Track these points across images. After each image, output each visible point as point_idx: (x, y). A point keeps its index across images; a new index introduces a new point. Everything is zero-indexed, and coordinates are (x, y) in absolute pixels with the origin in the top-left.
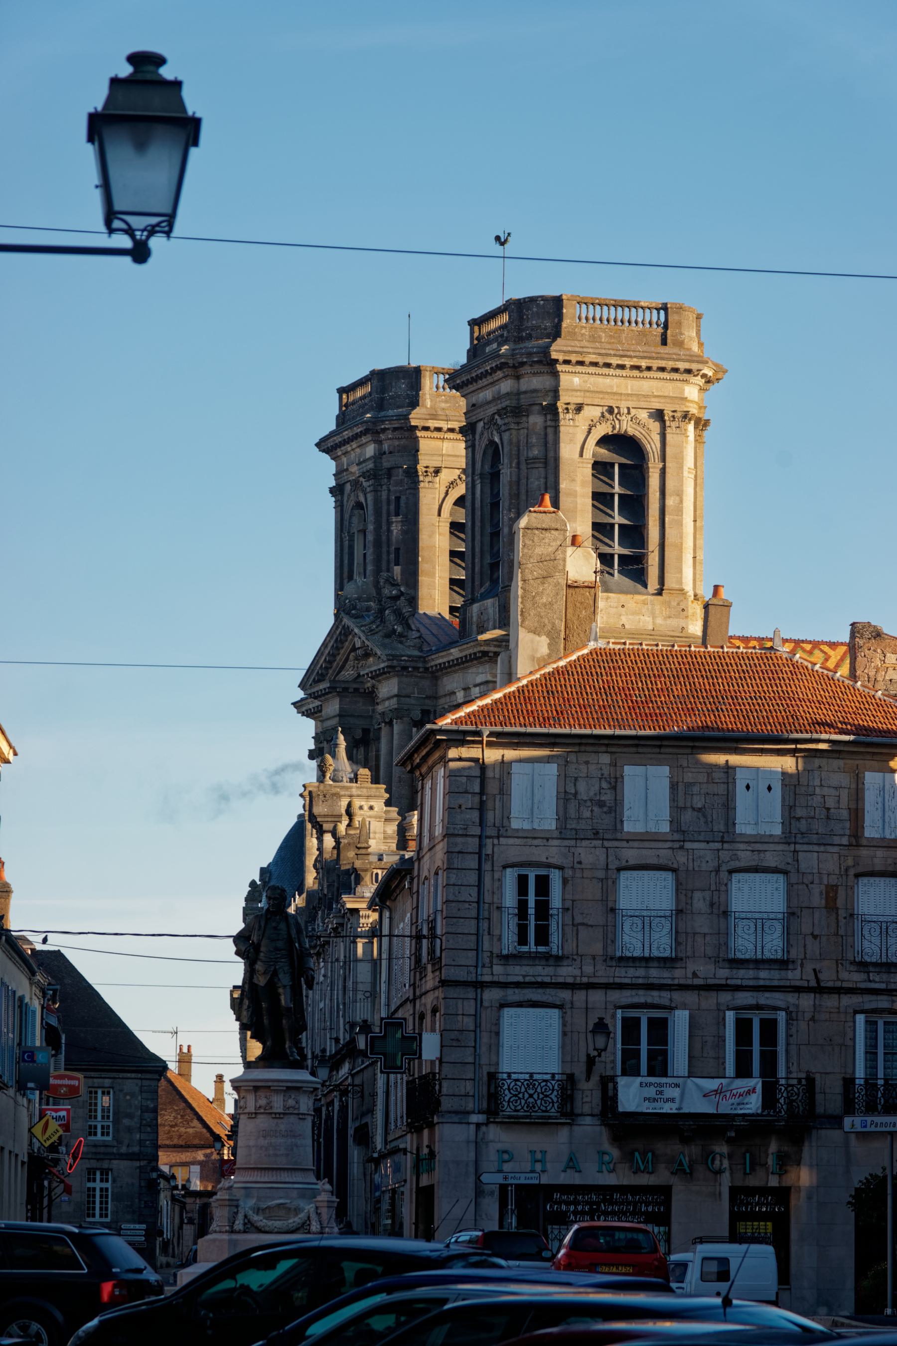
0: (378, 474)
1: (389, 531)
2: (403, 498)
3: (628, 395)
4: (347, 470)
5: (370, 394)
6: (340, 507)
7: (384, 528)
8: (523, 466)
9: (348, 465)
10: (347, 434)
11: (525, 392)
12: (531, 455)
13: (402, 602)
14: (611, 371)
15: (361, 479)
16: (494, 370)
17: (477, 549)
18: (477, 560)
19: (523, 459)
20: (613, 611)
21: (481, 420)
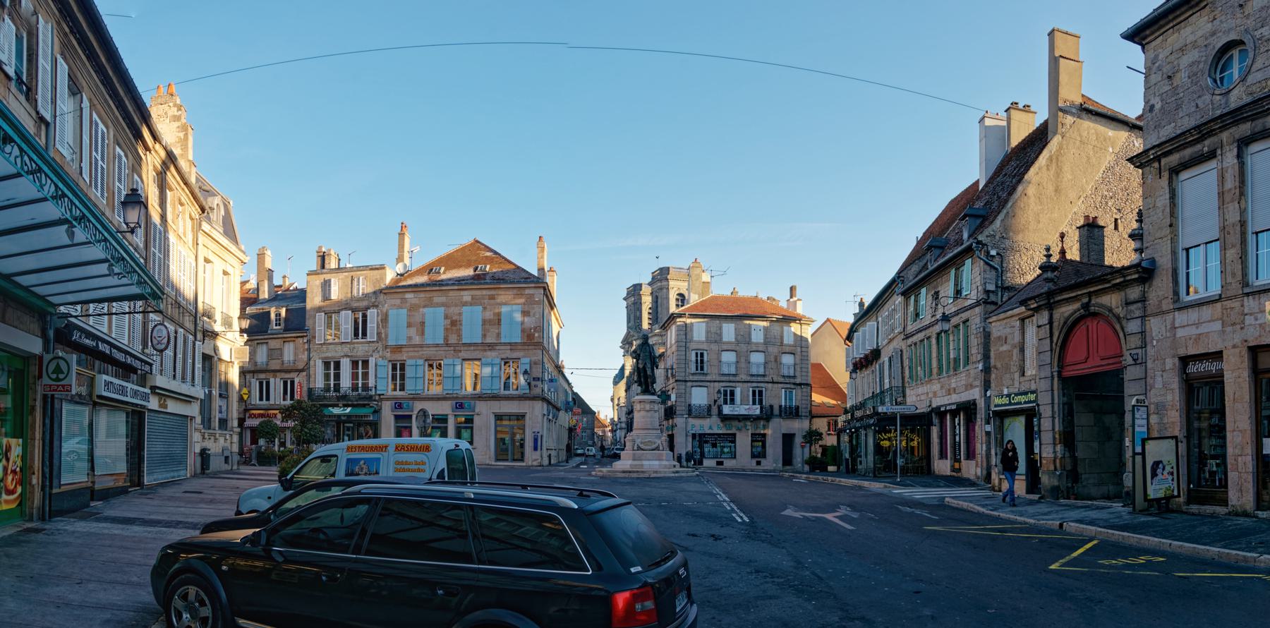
0: (635, 303)
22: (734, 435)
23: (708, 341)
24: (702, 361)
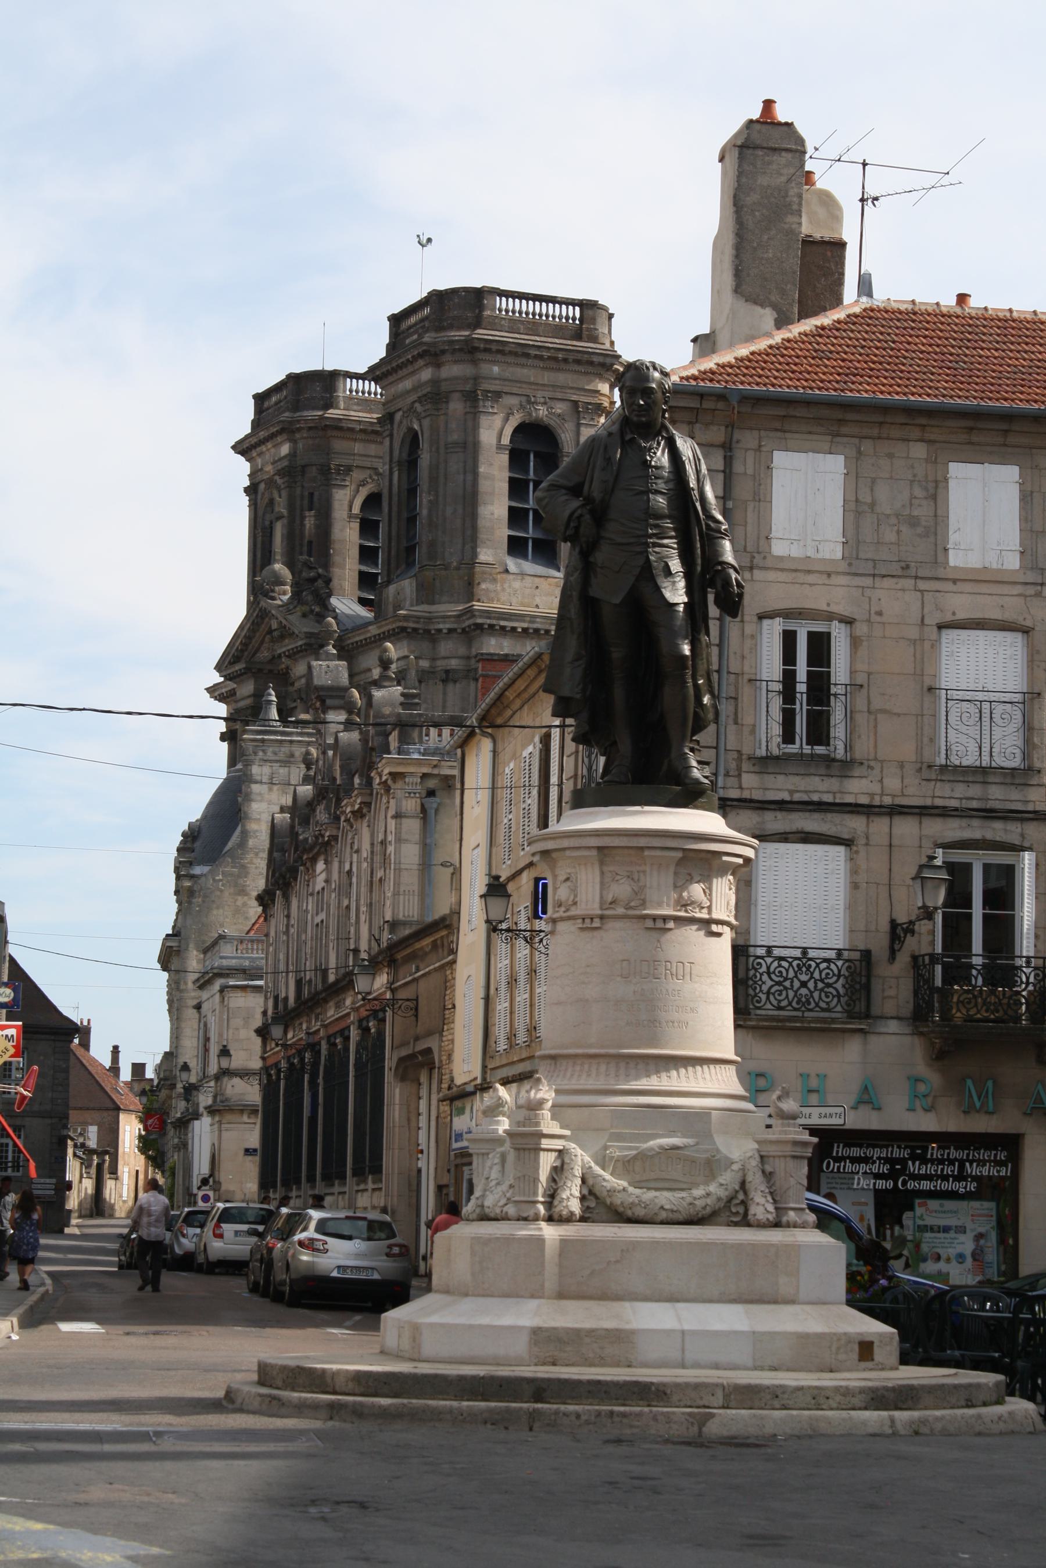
0: (292, 471)
1: (302, 525)
2: (316, 494)
3: (544, 385)
4: (261, 469)
5: (286, 397)
6: (254, 505)
7: (298, 522)
8: (442, 450)
9: (263, 465)
10: (262, 434)
11: (446, 380)
12: (450, 439)
13: (320, 583)
14: (530, 362)
15: (277, 478)
16: (415, 359)
17: (394, 533)
18: (393, 544)
20: (527, 591)
21: (399, 410)
22: (1010, 1145)
23: (860, 560)
24: (820, 687)
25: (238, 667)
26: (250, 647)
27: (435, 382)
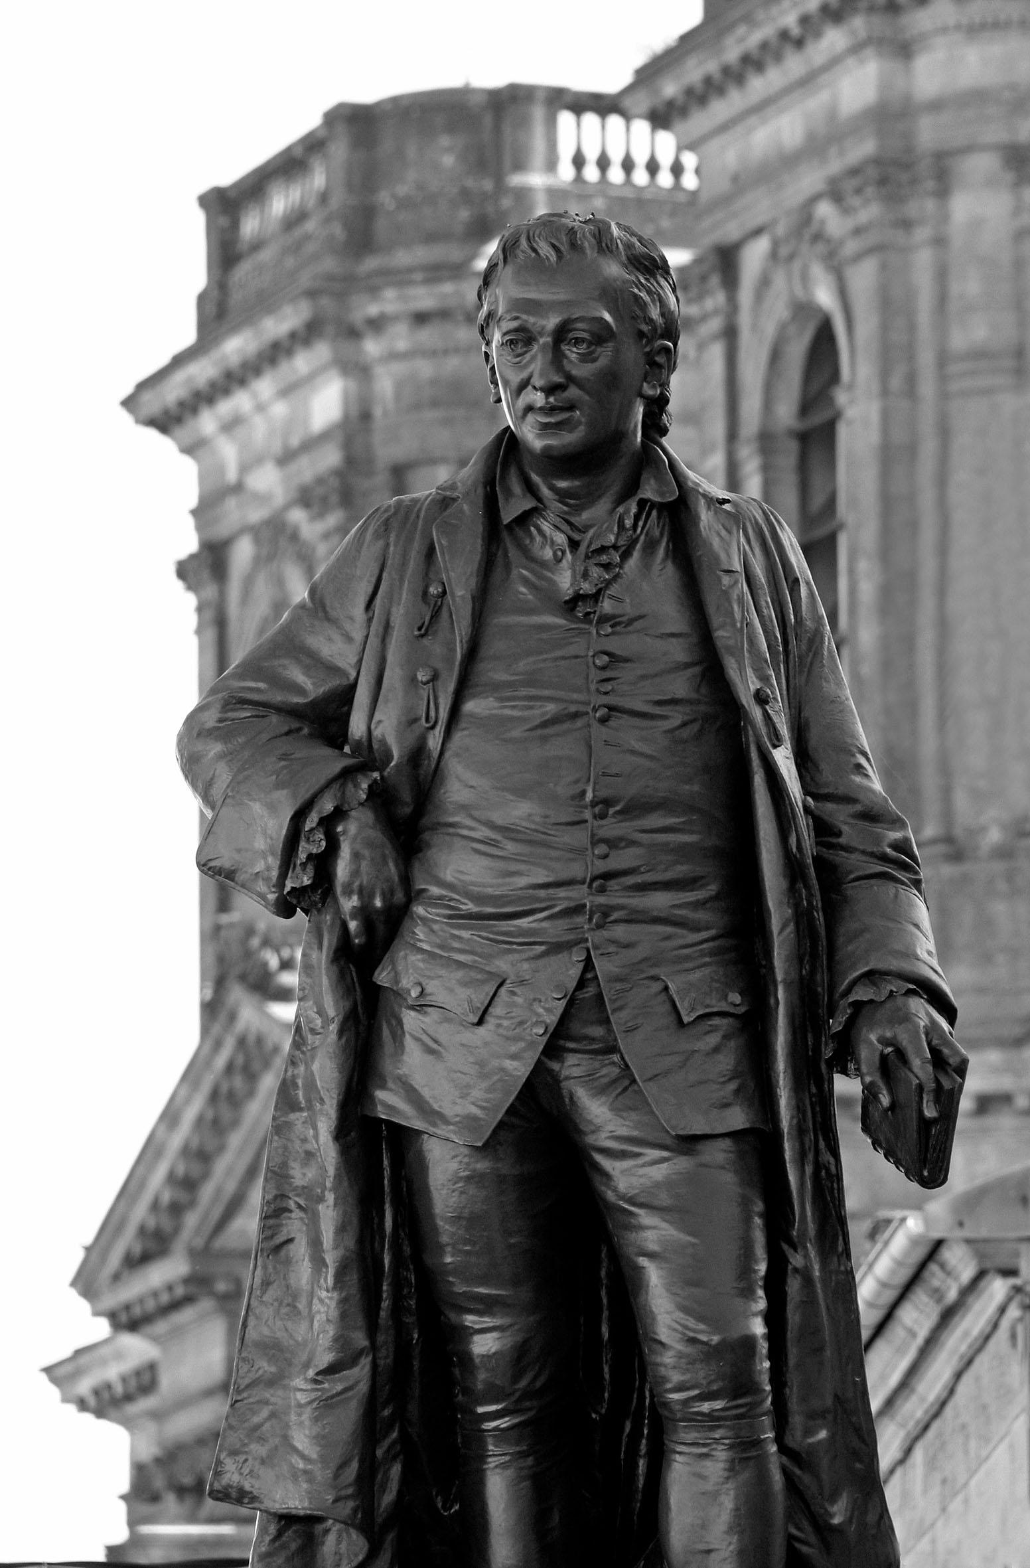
4: (238, 488)
5: (324, 198)
9: (245, 468)
10: (236, 346)
11: (936, 105)
12: (959, 340)
15: (297, 516)
19: (926, 358)
21: (758, 232)
25: (168, 1271)
26: (207, 1192)
27: (891, 115)
